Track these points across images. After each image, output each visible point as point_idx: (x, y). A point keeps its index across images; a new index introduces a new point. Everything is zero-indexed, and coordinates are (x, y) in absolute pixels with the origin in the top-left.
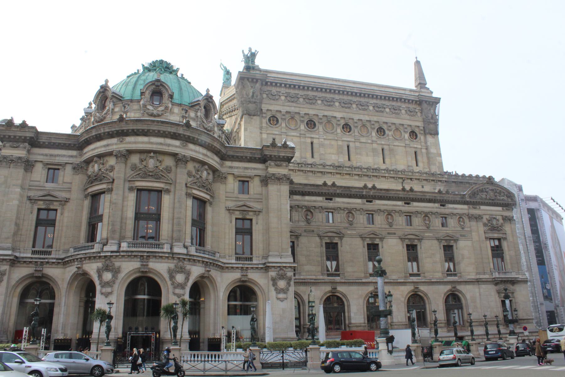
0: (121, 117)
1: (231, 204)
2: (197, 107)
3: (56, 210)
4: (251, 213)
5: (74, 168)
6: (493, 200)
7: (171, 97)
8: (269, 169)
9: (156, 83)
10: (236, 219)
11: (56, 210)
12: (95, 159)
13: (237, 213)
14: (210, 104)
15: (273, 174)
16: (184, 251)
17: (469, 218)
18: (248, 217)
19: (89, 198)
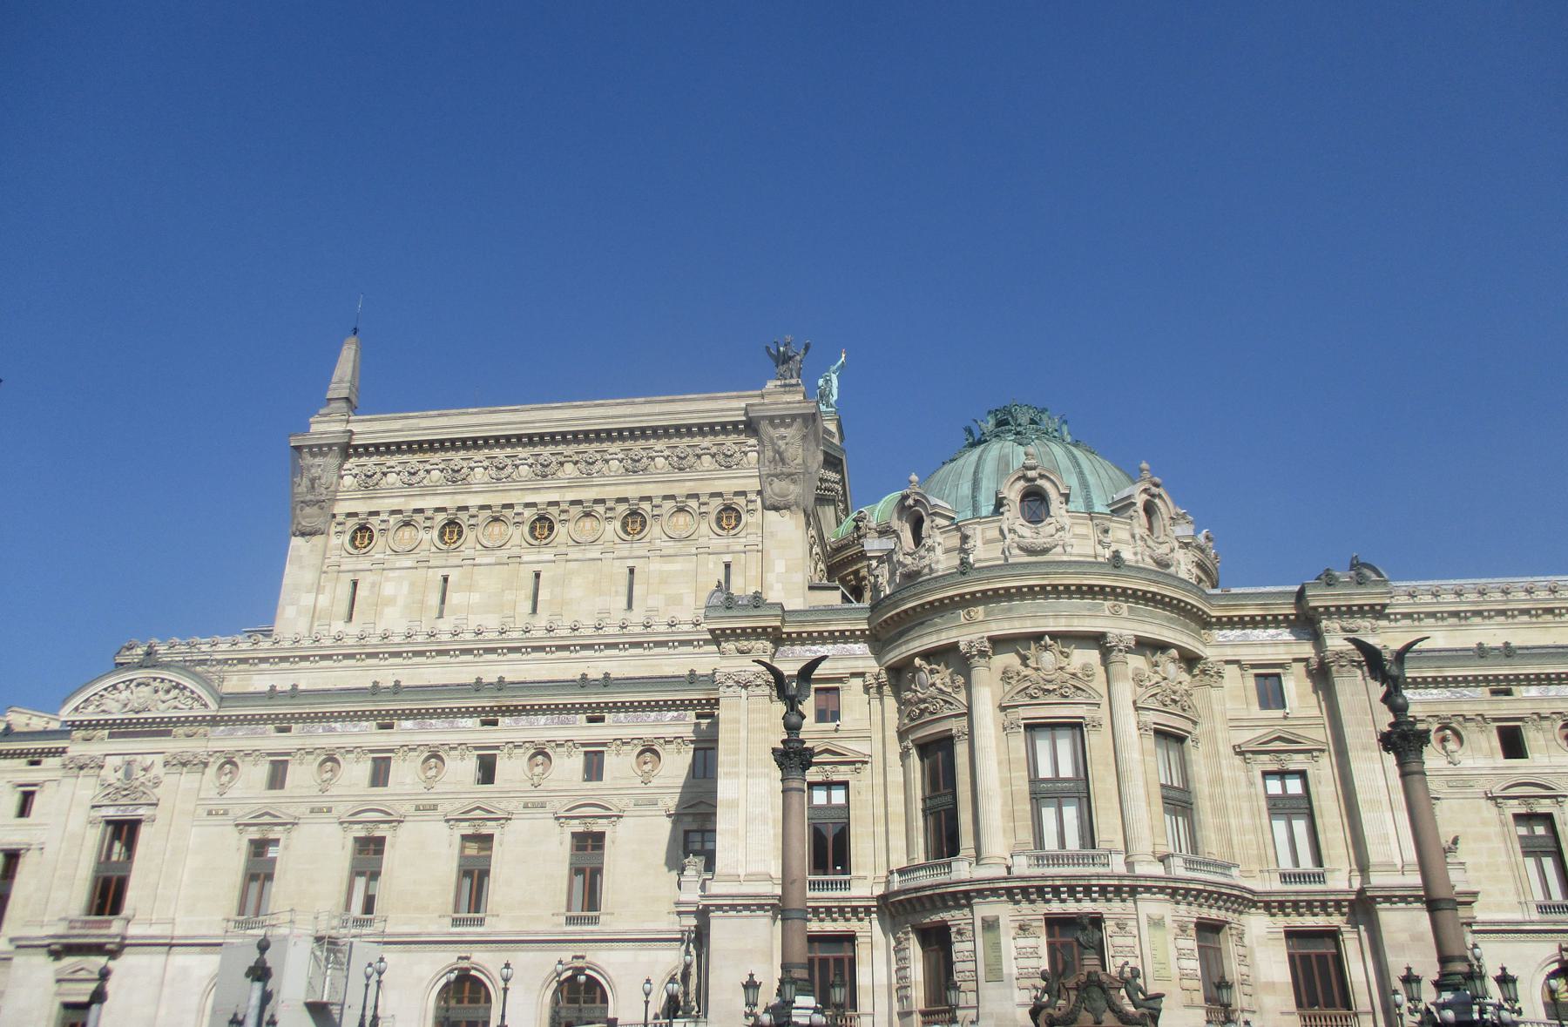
1: (1244, 737)
2: (1131, 512)
3: (845, 784)
4: (1301, 757)
7: (1067, 497)
9: (1031, 474)
10: (1266, 774)
11: (845, 784)
12: (917, 661)
16: (1158, 870)
18: (1292, 767)
19: (914, 752)
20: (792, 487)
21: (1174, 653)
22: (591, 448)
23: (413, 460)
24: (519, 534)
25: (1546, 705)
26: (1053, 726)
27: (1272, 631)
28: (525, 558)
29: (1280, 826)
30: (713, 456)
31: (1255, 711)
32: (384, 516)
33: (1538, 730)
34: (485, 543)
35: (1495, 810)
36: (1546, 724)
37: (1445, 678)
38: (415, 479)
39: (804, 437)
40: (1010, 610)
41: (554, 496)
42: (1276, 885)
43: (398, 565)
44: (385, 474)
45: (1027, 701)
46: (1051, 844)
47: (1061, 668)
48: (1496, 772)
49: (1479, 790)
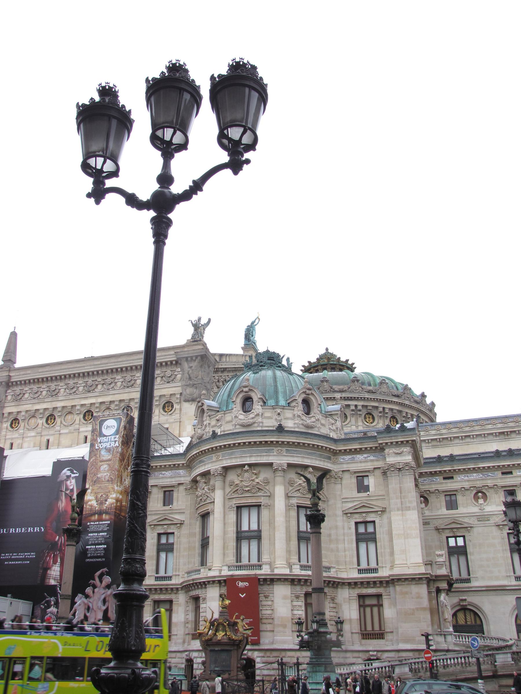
0: (214, 432)
4: (373, 515)
5: (186, 489)
8: (387, 460)
13: (357, 516)
14: (311, 397)
15: (392, 465)
16: (287, 571)
18: (369, 519)
20: (195, 390)
21: (311, 469)
22: (109, 378)
23: (35, 387)
24: (78, 418)
26: (249, 507)
27: (365, 455)
28: (81, 429)
29: (363, 546)
30: (162, 377)
31: (354, 493)
32: (23, 413)
34: (64, 423)
37: (479, 468)
38: (37, 395)
39: (201, 366)
40: (232, 454)
41: (93, 401)
42: (354, 575)
43: (29, 435)
44: (24, 394)
45: (237, 496)
46: (245, 561)
47: (253, 480)
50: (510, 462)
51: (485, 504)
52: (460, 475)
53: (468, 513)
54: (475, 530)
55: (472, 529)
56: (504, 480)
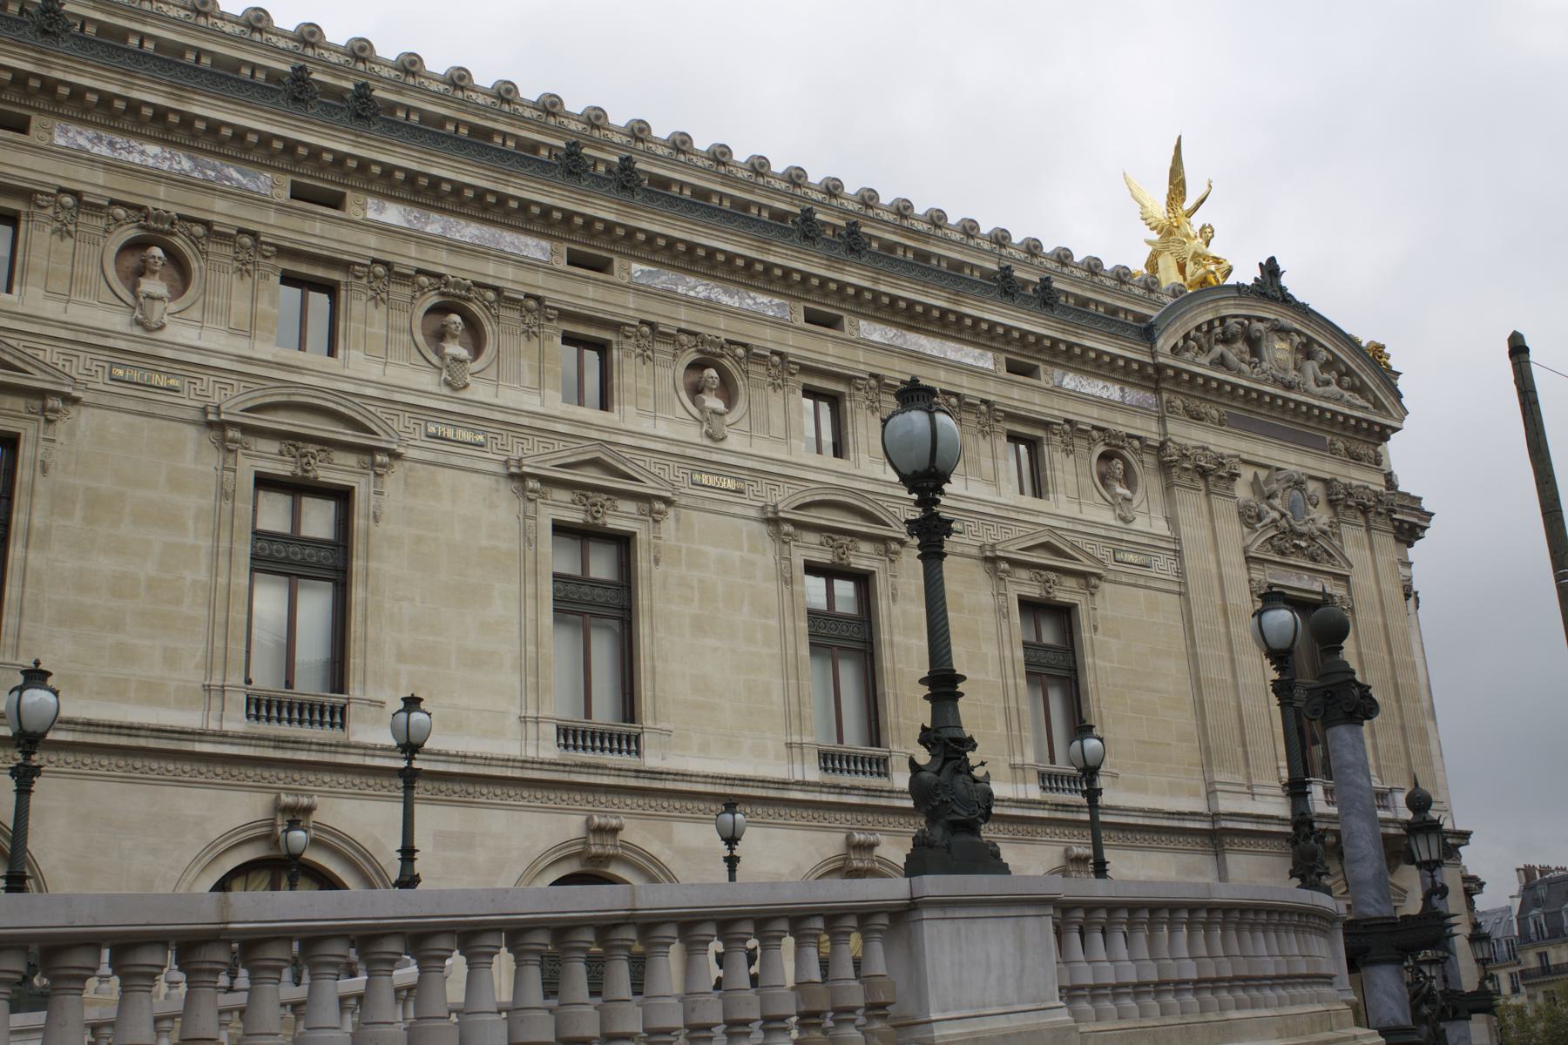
6: (1289, 387)
17: (1165, 467)
25: (412, 250)
33: (376, 299)
35: (213, 458)
36: (400, 292)
48: (243, 371)
49: (189, 401)
50: (356, 144)
51: (173, 307)
52: (73, 129)
53: (65, 325)
54: (84, 419)
55: (73, 410)
56: (294, 222)
